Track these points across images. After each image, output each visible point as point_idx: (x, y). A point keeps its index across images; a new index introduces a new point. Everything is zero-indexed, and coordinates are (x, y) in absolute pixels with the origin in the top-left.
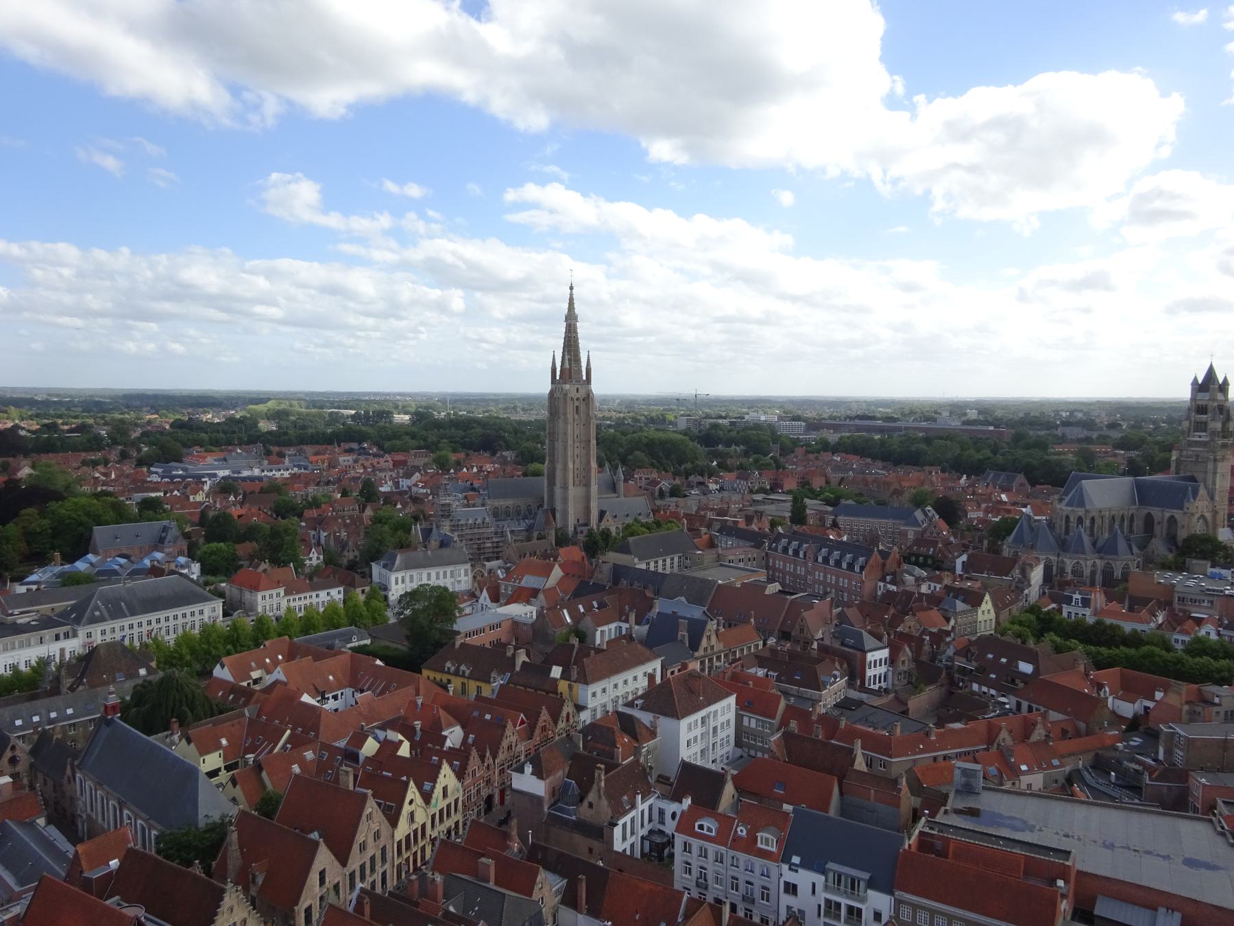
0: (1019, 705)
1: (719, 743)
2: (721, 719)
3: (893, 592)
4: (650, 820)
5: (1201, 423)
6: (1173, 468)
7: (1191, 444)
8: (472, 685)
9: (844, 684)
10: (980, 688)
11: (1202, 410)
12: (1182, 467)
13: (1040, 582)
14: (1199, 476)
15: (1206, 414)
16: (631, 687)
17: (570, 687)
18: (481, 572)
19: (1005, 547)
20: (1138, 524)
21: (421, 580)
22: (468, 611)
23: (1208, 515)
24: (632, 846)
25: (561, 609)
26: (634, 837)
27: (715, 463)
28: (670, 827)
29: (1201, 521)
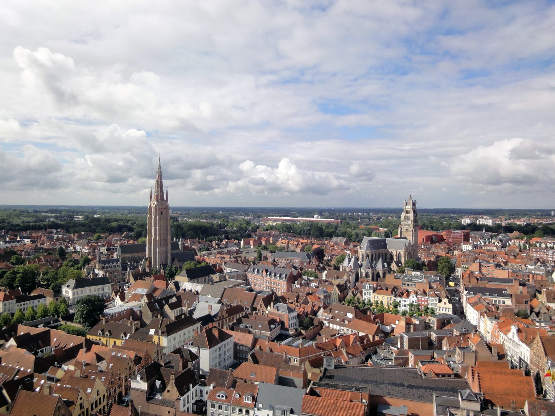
0: (348, 330)
1: (226, 358)
2: (227, 347)
3: (298, 288)
4: (196, 396)
8: (112, 341)
9: (280, 328)
10: (333, 326)
11: (408, 212)
13: (354, 280)
16: (187, 336)
17: (159, 338)
18: (116, 288)
20: (388, 256)
21: (86, 293)
22: (109, 306)
23: (412, 252)
24: (188, 408)
25: (154, 303)
26: (189, 404)
27: (223, 236)
28: (205, 398)
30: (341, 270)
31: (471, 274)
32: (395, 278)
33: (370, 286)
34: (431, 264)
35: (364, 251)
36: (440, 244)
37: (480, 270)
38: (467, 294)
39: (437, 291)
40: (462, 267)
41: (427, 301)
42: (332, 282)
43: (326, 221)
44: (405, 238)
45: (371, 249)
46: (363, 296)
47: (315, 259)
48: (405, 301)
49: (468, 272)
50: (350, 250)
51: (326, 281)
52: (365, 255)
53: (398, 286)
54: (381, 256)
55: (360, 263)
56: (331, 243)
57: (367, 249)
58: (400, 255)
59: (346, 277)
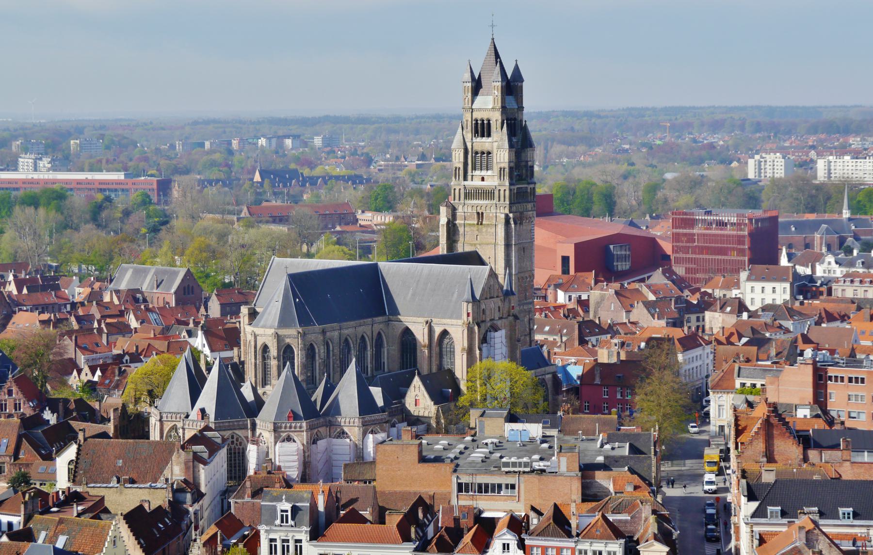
5: (483, 153)
7: (470, 194)
11: (482, 129)
14: (484, 255)
15: (489, 135)
20: (391, 352)
30: (155, 435)
31: (774, 420)
32: (423, 459)
33: (295, 510)
34: (598, 381)
35: (272, 331)
36: (642, 280)
37: (820, 398)
38: (753, 516)
39: (616, 511)
40: (738, 386)
42: (102, 499)
43: (79, 182)
44: (474, 259)
45: (304, 320)
47: (15, 389)
49: (761, 411)
50: (208, 333)
51: (73, 497)
52: (273, 351)
53: (433, 497)
54: (353, 352)
55: (249, 396)
56: (107, 299)
57: (284, 322)
58: (446, 341)
59: (176, 471)
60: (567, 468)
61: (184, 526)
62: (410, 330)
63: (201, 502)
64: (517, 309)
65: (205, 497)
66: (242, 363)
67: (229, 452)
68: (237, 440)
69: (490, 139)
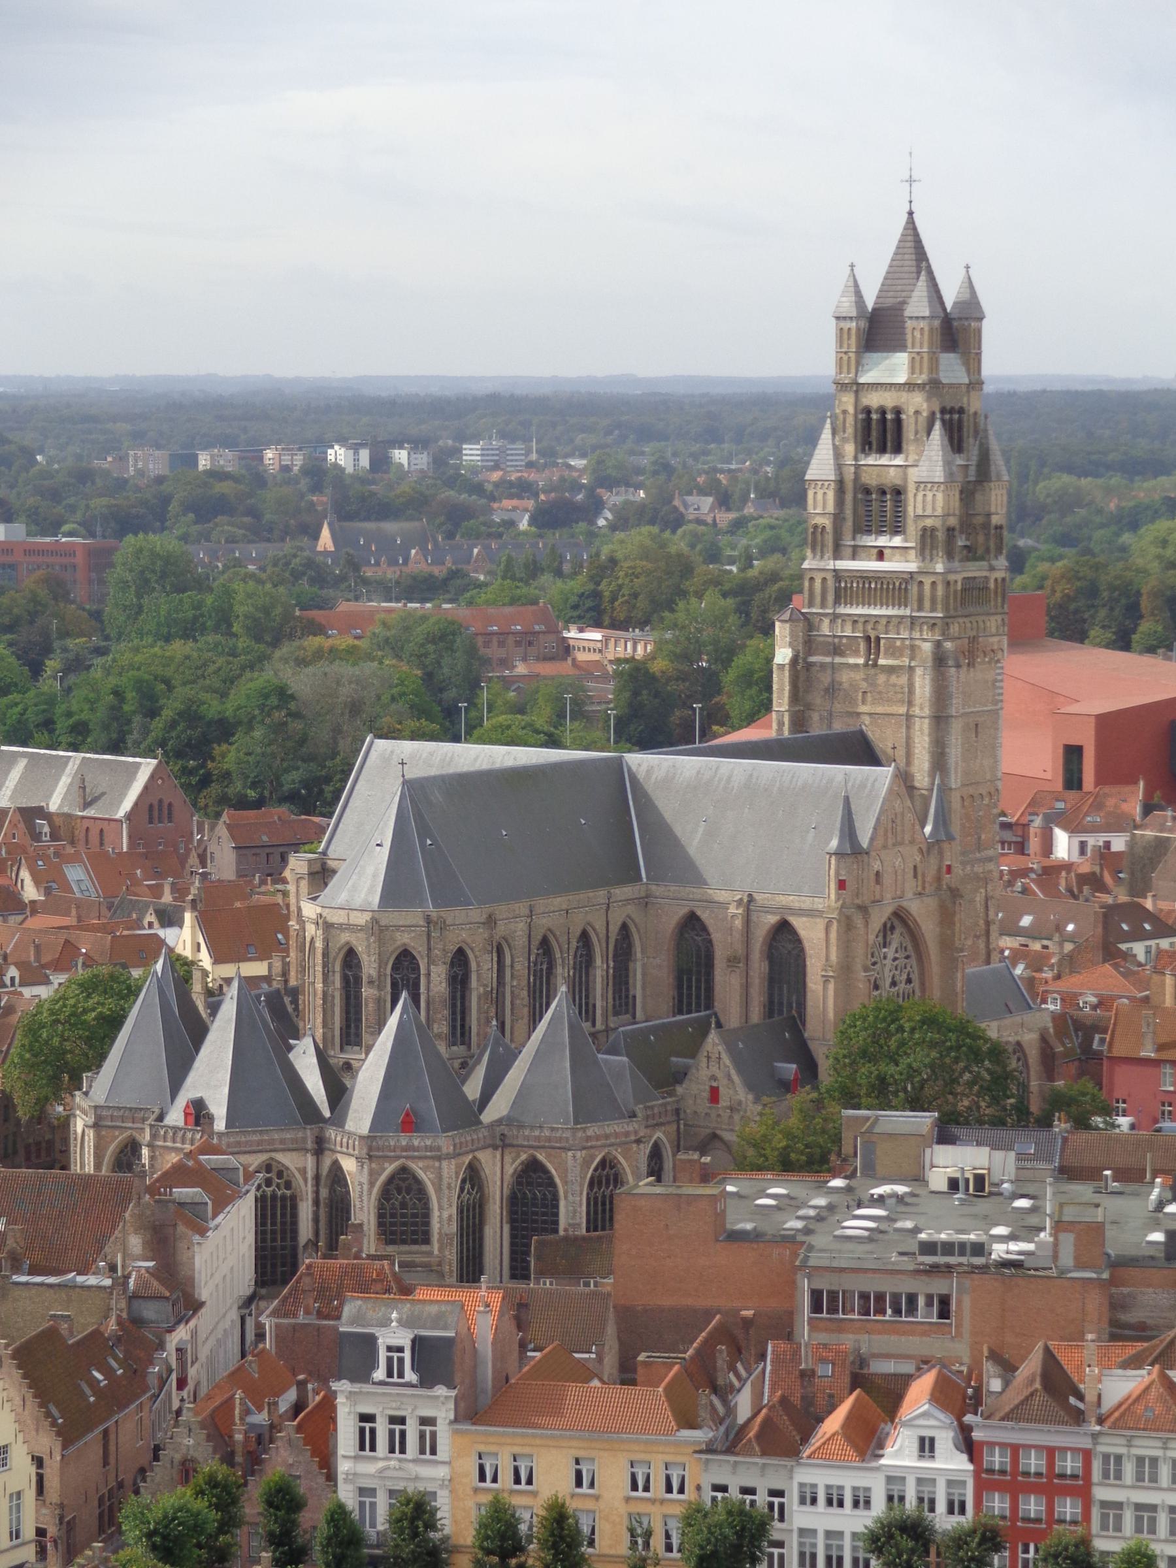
6: (781, 701)
12: (817, 699)
13: (245, 1277)
14: (883, 738)
15: (898, 449)
19: (79, 1124)
23: (922, 911)
29: (896, 939)
35: (367, 917)
41: (1081, 1489)
46: (344, 1467)
48: (835, 1500)
60: (1076, 1258)
61: (153, 1381)
62: (698, 919)
63: (192, 1324)
64: (958, 870)
65: (203, 1310)
66: (295, 993)
67: (261, 1201)
68: (280, 1175)
69: (899, 460)
